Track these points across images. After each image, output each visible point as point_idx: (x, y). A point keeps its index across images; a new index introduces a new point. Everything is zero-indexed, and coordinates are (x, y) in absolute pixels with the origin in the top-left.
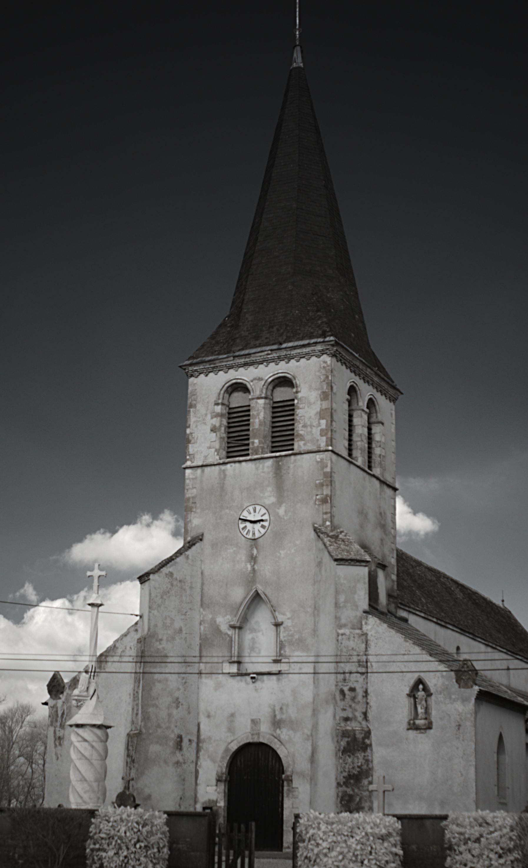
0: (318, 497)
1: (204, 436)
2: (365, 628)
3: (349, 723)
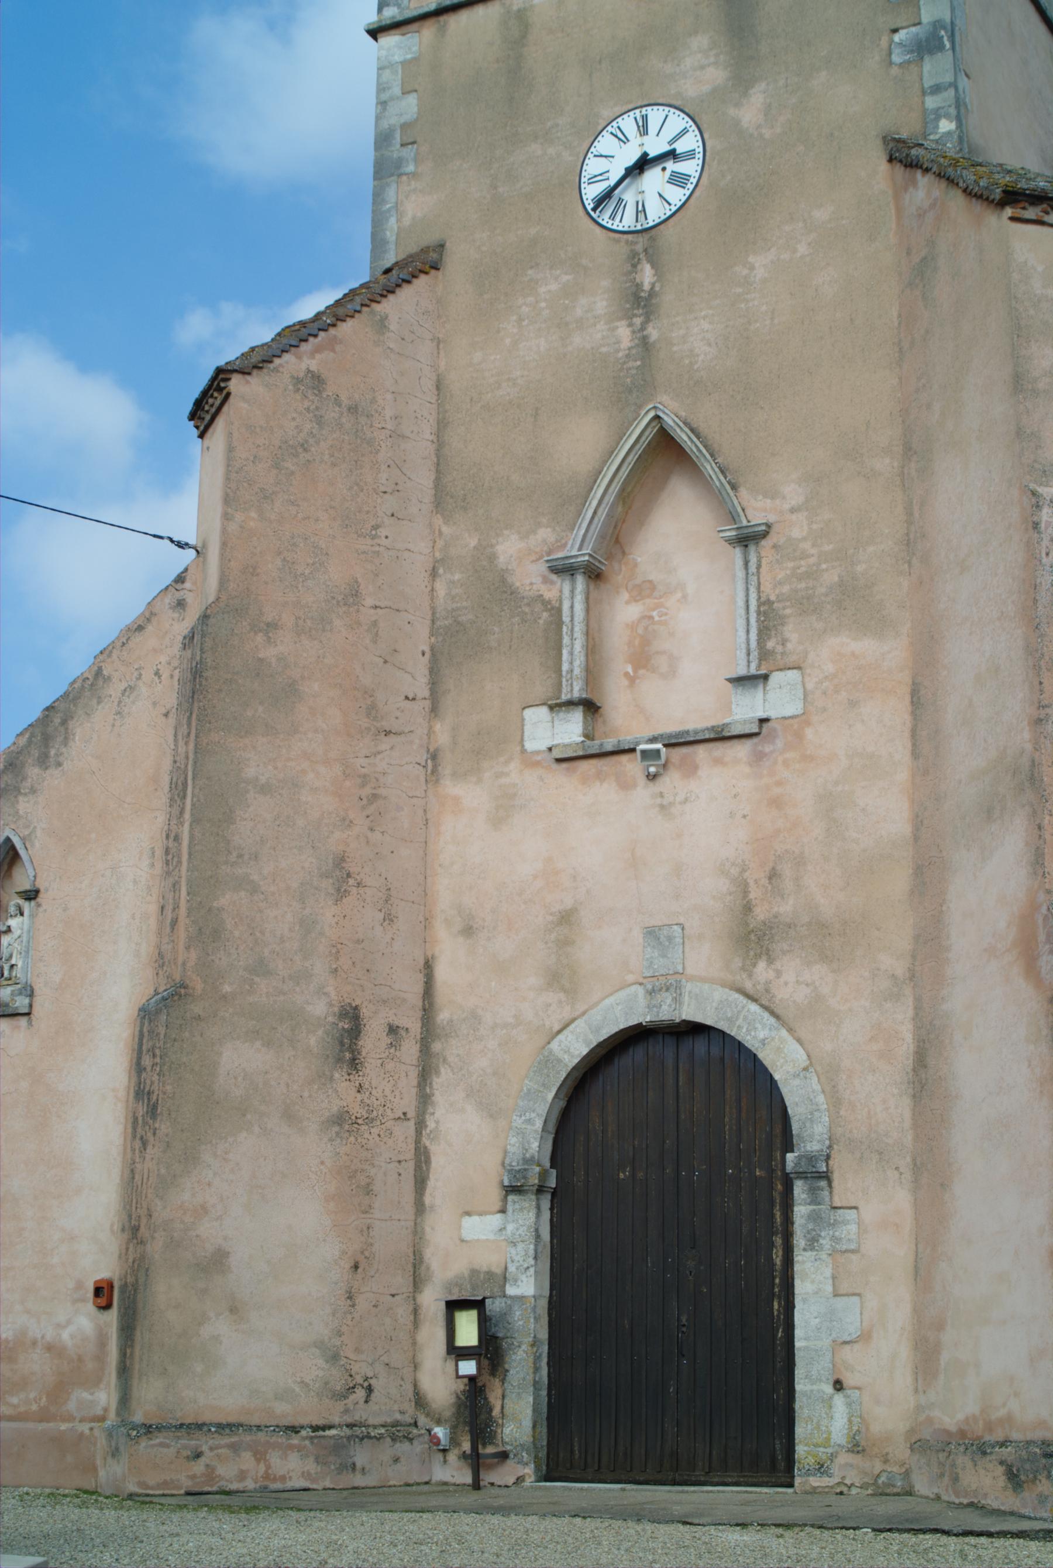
0: (897, 38)
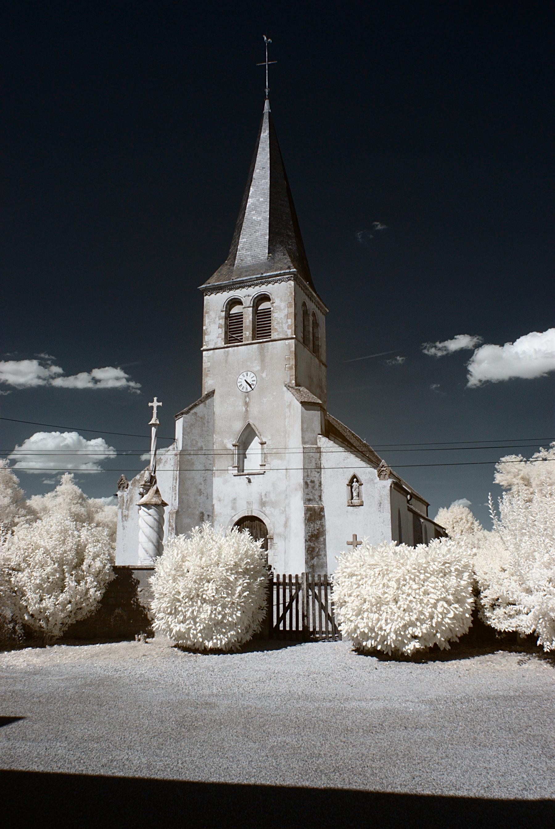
1: (213, 330)
2: (319, 444)
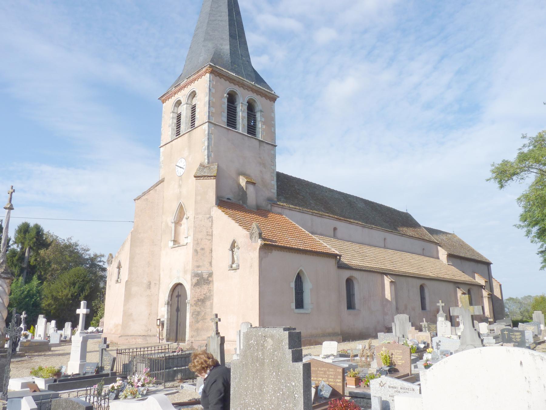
3: (200, 269)
